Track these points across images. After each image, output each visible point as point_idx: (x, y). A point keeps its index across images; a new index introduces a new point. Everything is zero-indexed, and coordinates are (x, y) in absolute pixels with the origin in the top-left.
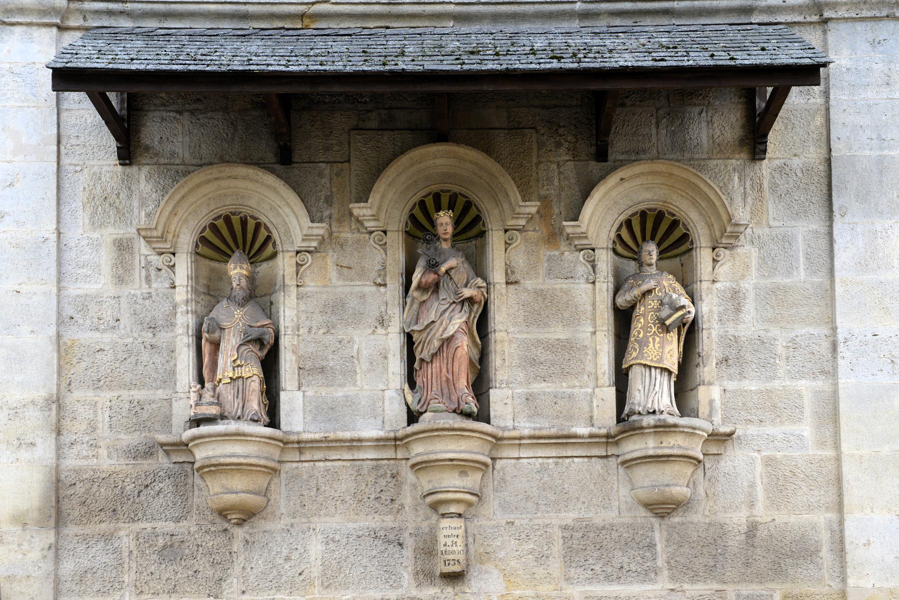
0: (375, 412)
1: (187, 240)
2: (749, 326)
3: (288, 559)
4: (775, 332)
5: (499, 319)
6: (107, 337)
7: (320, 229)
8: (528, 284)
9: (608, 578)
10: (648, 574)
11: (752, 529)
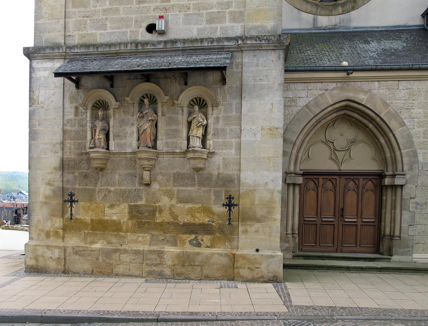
0: (131, 146)
1: (90, 106)
3: (111, 179)
4: (227, 127)
5: (159, 124)
6: (73, 128)
7: (118, 103)
8: (167, 115)
9: (184, 186)
10: (193, 185)
11: (219, 174)
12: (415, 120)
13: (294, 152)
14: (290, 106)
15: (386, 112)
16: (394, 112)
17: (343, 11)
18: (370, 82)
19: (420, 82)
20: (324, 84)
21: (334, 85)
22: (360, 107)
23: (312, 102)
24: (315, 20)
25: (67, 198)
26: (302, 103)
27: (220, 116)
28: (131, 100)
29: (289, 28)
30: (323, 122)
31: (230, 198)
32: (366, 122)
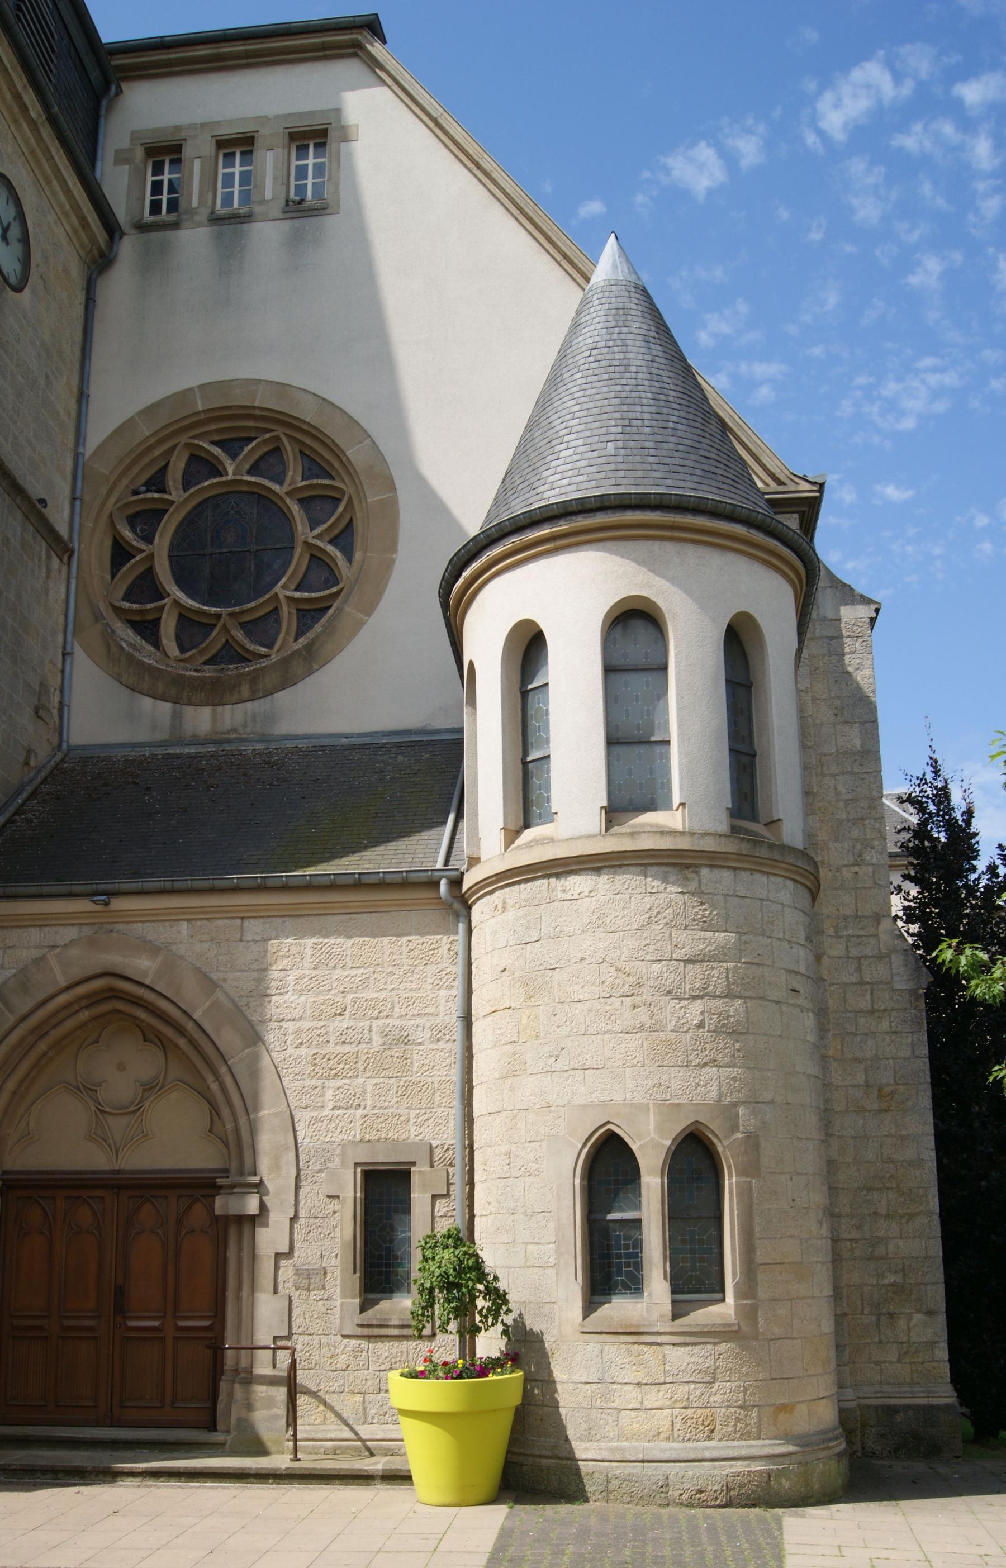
12: (284, 1024)
15: (207, 1004)
16: (229, 1005)
18: (167, 924)
20: (46, 929)
21: (72, 933)
24: (177, 718)
30: (54, 1035)
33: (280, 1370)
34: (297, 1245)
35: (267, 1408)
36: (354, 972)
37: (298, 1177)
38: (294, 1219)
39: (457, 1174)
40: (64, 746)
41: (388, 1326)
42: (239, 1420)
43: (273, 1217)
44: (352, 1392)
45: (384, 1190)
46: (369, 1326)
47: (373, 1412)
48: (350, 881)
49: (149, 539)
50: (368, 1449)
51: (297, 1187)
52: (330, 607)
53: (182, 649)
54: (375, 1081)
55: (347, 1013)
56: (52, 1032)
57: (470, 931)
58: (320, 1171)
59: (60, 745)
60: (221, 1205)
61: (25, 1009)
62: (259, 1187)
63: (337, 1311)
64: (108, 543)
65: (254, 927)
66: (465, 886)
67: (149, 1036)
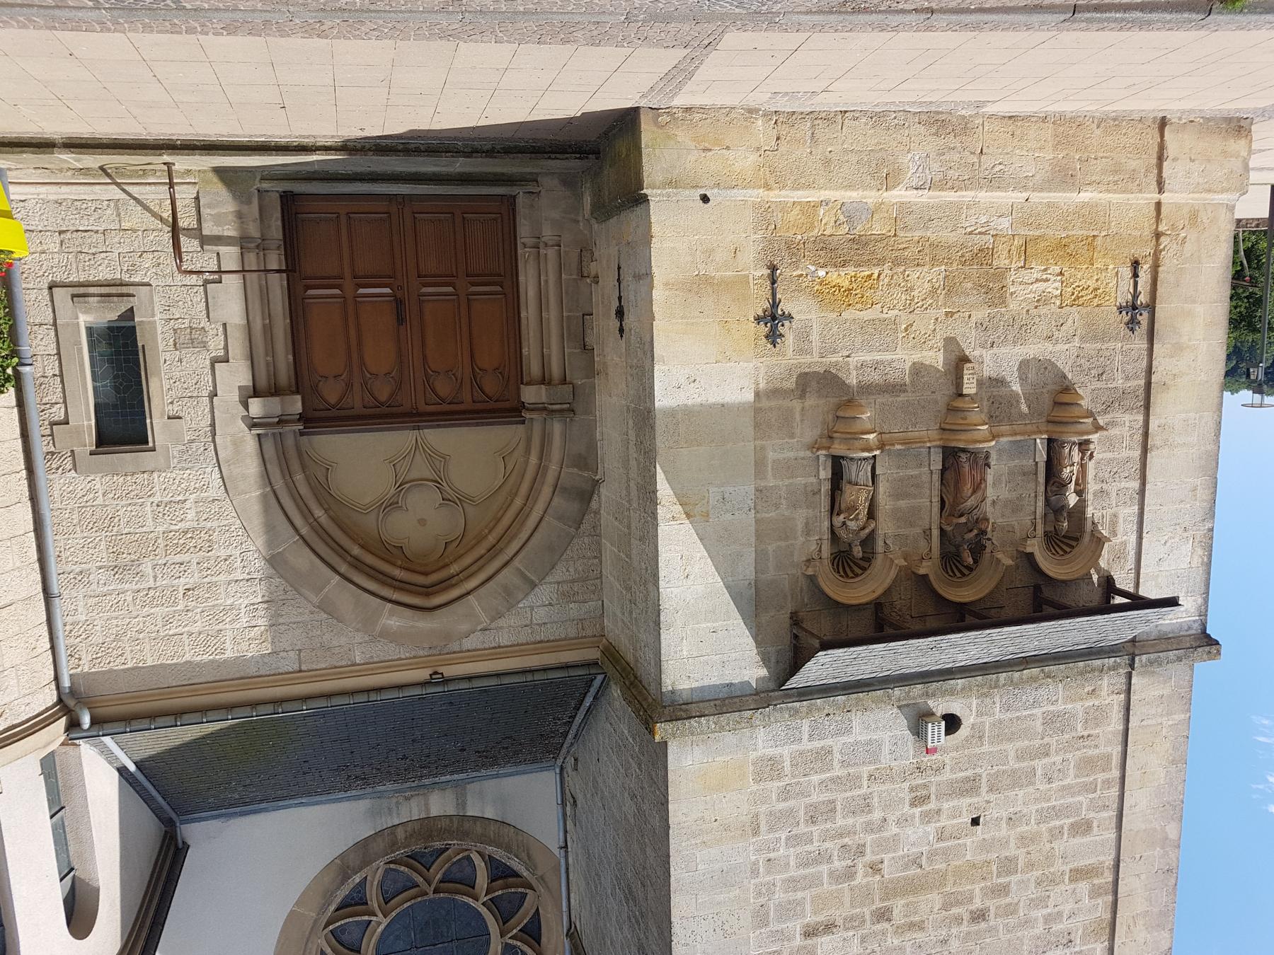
1: (1087, 538)
2: (801, 515)
8: (919, 530)
9: (882, 362)
13: (554, 468)
14: (573, 581)
16: (303, 591)
17: (393, 833)
19: (242, 674)
20: (494, 645)
21: (468, 644)
22: (396, 596)
23: (521, 596)
24: (462, 804)
25: (1144, 318)
26: (545, 593)
27: (802, 539)
28: (998, 561)
29: (525, 777)
31: (773, 337)
32: (370, 559)
33: (212, 251)
34: (208, 370)
35: (222, 214)
36: (179, 630)
37: (214, 435)
38: (214, 394)
39: (41, 447)
40: (558, 770)
41: (101, 295)
42: (249, 202)
43: (235, 396)
44: (135, 231)
45: (123, 425)
46: (122, 295)
47: (109, 212)
48: (186, 718)
49: (507, 947)
50: (108, 175)
51: (213, 425)
52: (337, 910)
53: (468, 858)
54: (144, 529)
55: (181, 591)
56: (483, 551)
57: (57, 678)
58: (192, 441)
59: (562, 769)
60: (296, 405)
61: (505, 571)
62: (253, 425)
63: (158, 309)
64: (544, 940)
65: (288, 663)
66: (62, 722)
67: (392, 552)
